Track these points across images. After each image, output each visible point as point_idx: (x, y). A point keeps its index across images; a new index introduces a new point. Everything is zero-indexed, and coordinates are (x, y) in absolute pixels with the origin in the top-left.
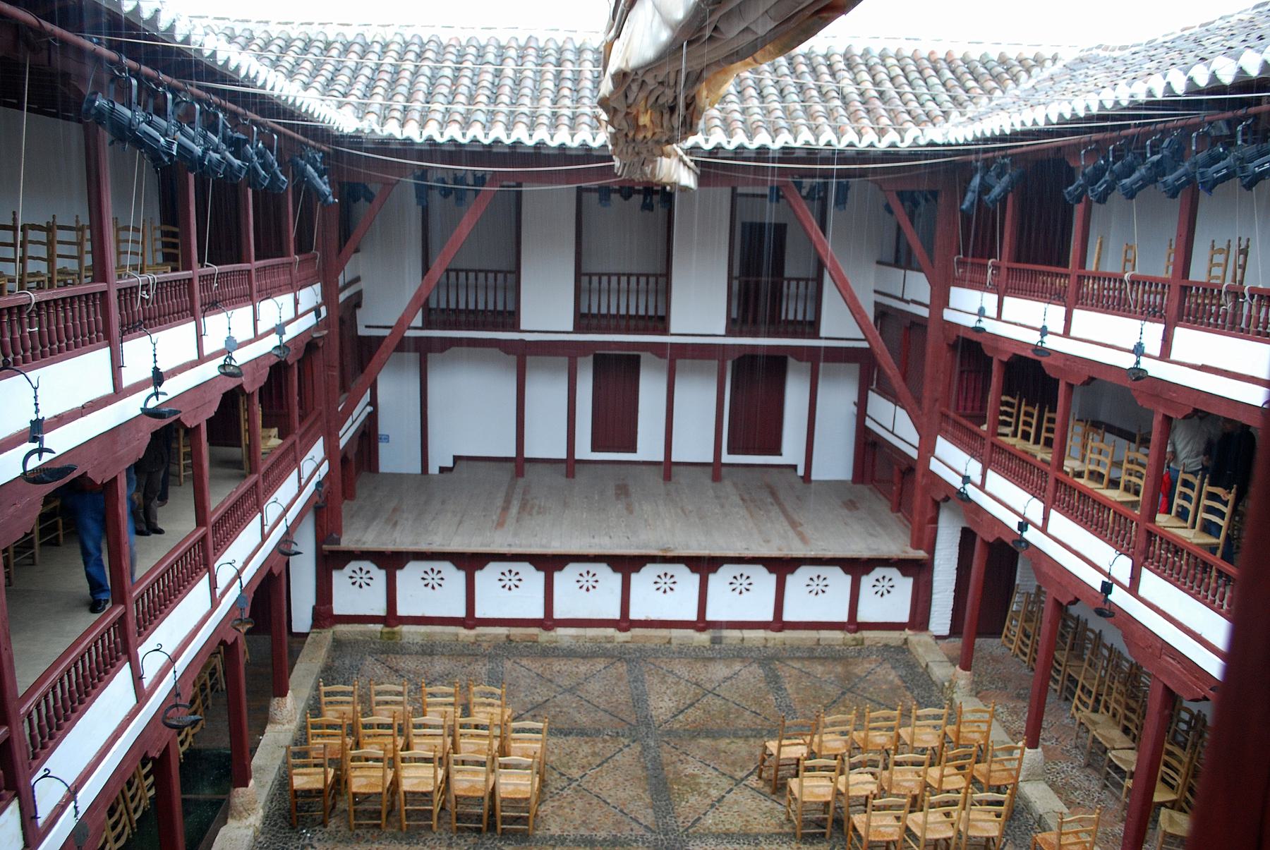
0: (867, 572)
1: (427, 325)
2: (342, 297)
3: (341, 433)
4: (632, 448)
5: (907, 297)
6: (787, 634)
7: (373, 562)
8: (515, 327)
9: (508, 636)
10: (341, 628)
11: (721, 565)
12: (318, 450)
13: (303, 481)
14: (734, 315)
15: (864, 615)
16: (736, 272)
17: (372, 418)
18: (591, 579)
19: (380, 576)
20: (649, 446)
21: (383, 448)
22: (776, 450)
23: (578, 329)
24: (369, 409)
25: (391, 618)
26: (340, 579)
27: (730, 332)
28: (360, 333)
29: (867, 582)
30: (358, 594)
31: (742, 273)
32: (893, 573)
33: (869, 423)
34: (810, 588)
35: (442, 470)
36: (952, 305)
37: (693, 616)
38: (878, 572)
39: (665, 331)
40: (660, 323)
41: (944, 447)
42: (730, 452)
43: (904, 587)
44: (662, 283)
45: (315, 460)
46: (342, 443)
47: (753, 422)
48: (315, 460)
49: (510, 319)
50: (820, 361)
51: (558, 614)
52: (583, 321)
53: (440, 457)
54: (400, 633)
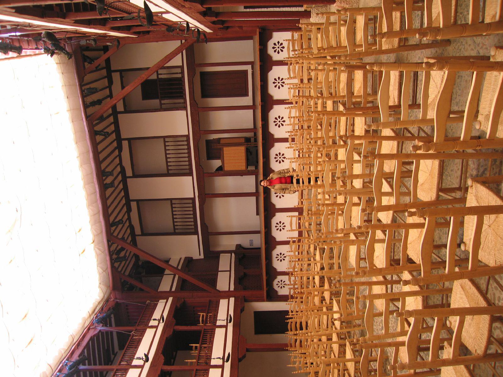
0: (270, 57)
7: (273, 280)
8: (193, 199)
19: (279, 278)
22: (246, 72)
28: (203, 257)
29: (276, 57)
38: (270, 51)
47: (234, 84)
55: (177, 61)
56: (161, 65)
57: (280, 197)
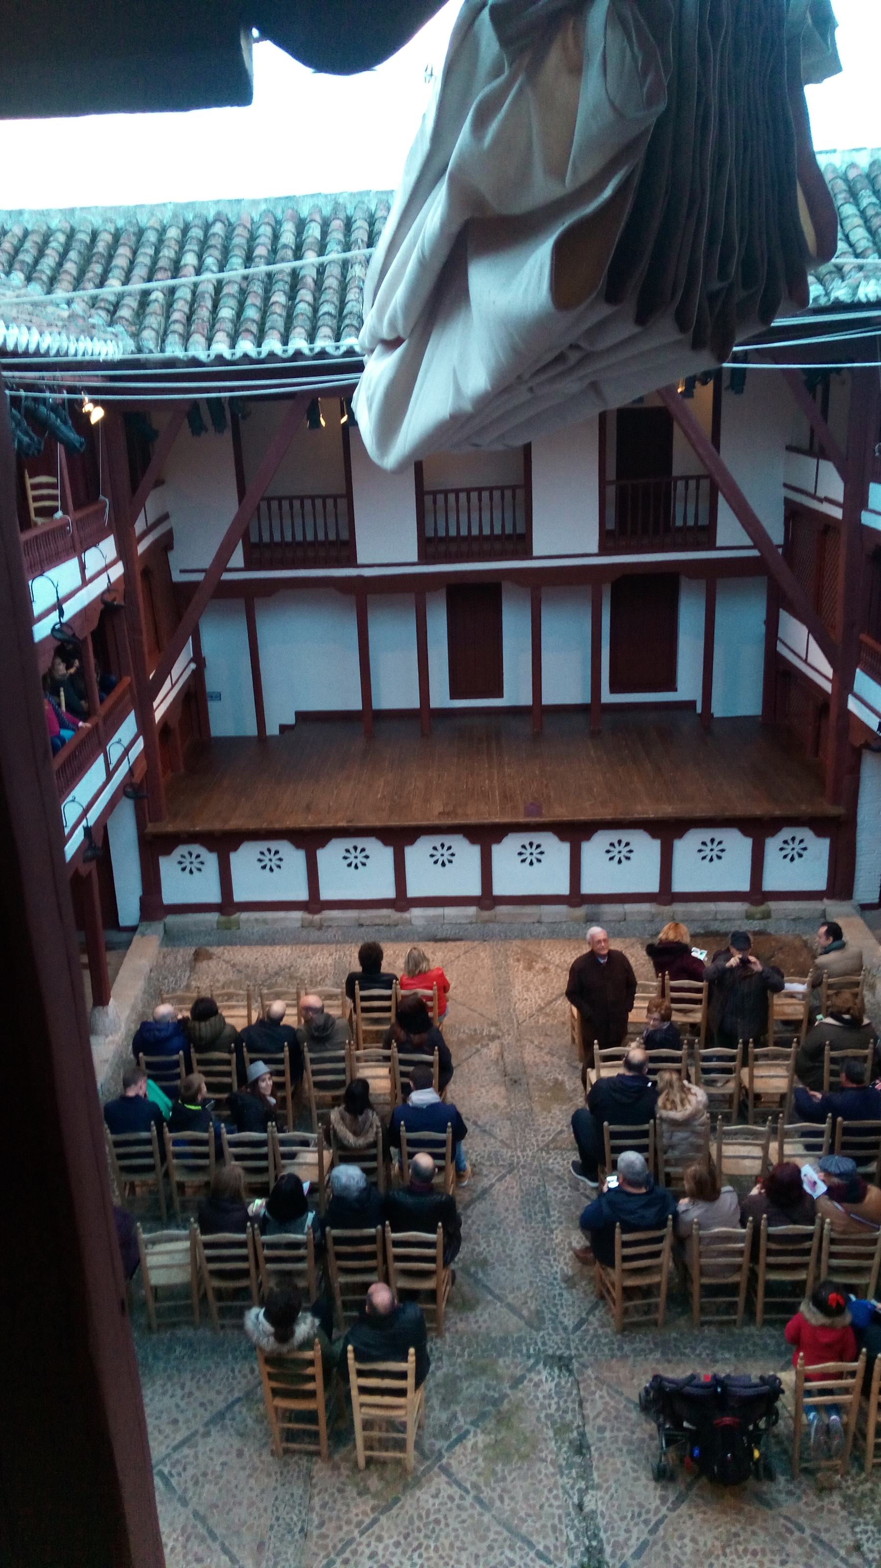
0: (773, 834)
1: (249, 566)
2: (141, 548)
3: (155, 704)
4: (499, 694)
5: (821, 494)
6: (679, 908)
9: (358, 919)
10: (170, 919)
11: (594, 831)
12: (128, 727)
13: (111, 767)
14: (610, 525)
15: (770, 884)
16: (611, 475)
17: (197, 678)
18: (447, 854)
19: (211, 860)
20: (516, 691)
21: (213, 707)
22: (671, 686)
23: (425, 557)
24: (193, 666)
25: (227, 905)
26: (168, 866)
27: (604, 550)
29: (772, 845)
30: (188, 880)
31: (620, 474)
32: (806, 834)
33: (781, 648)
34: (703, 854)
35: (283, 728)
36: (872, 505)
37: (564, 889)
38: (786, 833)
39: (527, 554)
40: (521, 543)
41: (862, 681)
42: (614, 689)
43: (819, 849)
44: (519, 495)
45: (126, 739)
46: (158, 715)
48: (126, 739)
49: (344, 551)
50: (717, 576)
51: (412, 892)
52: (429, 547)
53: (280, 714)
54: (238, 923)
55: (730, 534)
56: (716, 485)
57: (432, 856)
